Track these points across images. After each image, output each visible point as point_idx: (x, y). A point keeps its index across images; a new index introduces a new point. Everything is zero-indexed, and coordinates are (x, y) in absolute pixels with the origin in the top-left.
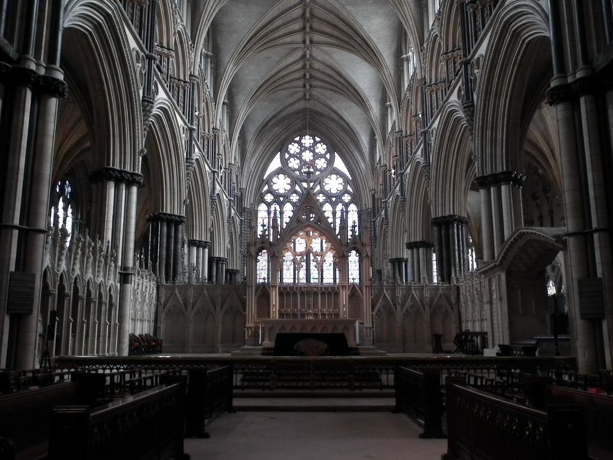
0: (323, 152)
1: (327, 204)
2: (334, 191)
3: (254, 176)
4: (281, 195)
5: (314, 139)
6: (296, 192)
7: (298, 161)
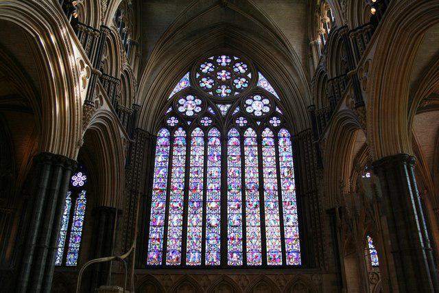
0: (242, 71)
1: (250, 129)
2: (258, 114)
3: (154, 93)
4: (189, 118)
5: (233, 59)
6: (208, 115)
7: (211, 81)
